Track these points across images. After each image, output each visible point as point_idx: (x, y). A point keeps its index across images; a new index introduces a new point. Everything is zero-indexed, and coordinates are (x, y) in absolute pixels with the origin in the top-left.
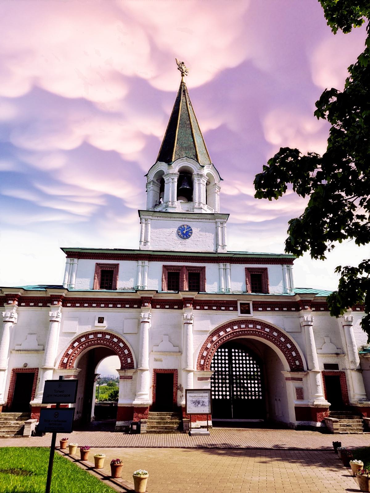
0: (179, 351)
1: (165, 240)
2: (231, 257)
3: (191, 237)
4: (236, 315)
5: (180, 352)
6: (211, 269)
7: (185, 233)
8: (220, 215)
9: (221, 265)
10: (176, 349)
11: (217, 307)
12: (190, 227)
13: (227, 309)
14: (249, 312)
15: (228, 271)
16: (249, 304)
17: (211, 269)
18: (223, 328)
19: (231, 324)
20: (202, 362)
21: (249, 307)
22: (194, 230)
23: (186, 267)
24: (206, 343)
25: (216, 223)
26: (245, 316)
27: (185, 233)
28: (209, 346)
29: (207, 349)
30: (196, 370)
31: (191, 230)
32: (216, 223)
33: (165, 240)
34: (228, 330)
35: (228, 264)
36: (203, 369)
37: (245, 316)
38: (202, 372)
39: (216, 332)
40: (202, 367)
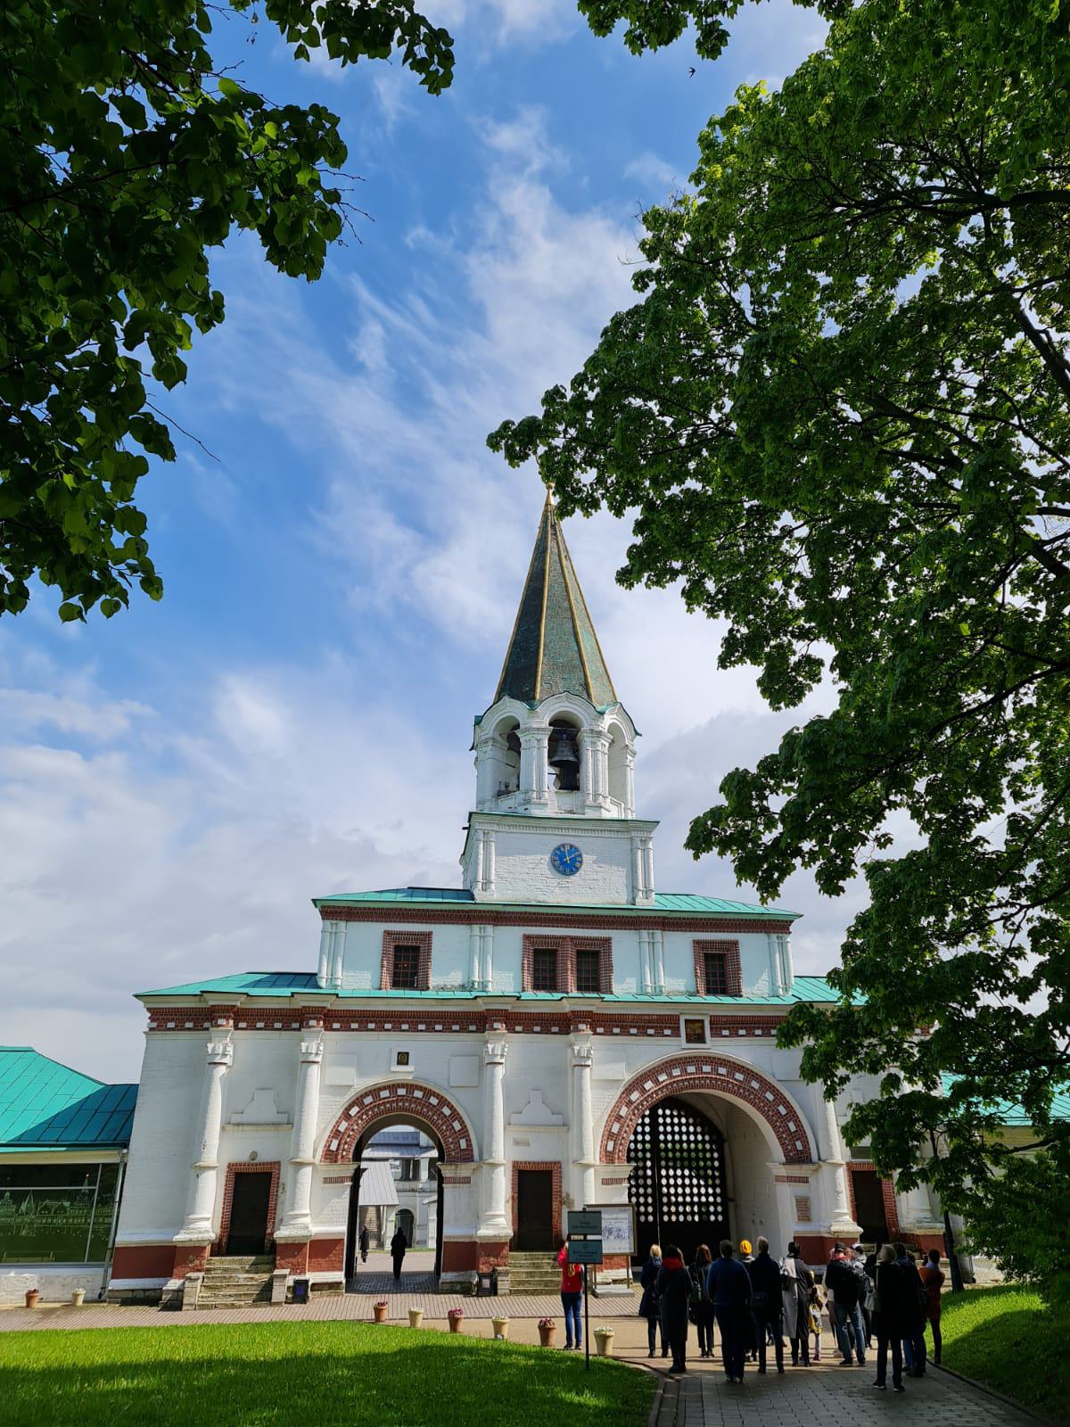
0: (564, 1121)
1: (525, 877)
2: (665, 918)
3: (581, 871)
4: (676, 1047)
5: (565, 1124)
6: (623, 944)
7: (566, 863)
8: (641, 824)
9: (644, 933)
10: (557, 1119)
11: (638, 1028)
12: (577, 850)
13: (659, 1033)
14: (700, 1038)
15: (659, 947)
16: (702, 1021)
17: (623, 944)
18: (651, 1074)
19: (667, 1066)
20: (610, 1147)
21: (702, 1028)
22: (587, 859)
23: (572, 938)
24: (617, 1106)
25: (631, 839)
26: (696, 1049)
27: (566, 863)
28: (624, 1111)
29: (619, 1118)
30: (598, 1162)
31: (580, 856)
32: (631, 839)
33: (525, 877)
34: (663, 1077)
35: (658, 933)
36: (612, 1161)
37: (696, 1049)
38: (611, 1168)
39: (637, 1084)
40: (609, 1157)
